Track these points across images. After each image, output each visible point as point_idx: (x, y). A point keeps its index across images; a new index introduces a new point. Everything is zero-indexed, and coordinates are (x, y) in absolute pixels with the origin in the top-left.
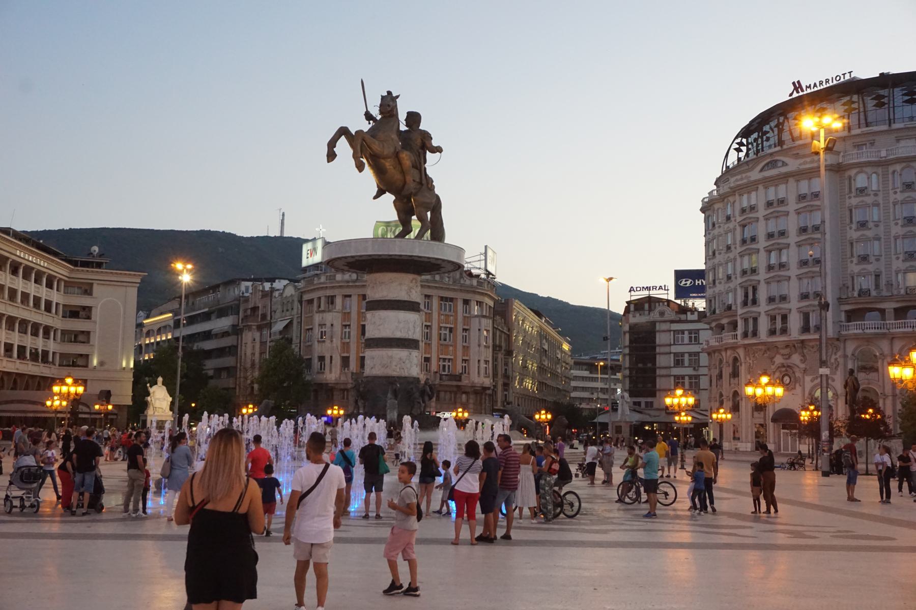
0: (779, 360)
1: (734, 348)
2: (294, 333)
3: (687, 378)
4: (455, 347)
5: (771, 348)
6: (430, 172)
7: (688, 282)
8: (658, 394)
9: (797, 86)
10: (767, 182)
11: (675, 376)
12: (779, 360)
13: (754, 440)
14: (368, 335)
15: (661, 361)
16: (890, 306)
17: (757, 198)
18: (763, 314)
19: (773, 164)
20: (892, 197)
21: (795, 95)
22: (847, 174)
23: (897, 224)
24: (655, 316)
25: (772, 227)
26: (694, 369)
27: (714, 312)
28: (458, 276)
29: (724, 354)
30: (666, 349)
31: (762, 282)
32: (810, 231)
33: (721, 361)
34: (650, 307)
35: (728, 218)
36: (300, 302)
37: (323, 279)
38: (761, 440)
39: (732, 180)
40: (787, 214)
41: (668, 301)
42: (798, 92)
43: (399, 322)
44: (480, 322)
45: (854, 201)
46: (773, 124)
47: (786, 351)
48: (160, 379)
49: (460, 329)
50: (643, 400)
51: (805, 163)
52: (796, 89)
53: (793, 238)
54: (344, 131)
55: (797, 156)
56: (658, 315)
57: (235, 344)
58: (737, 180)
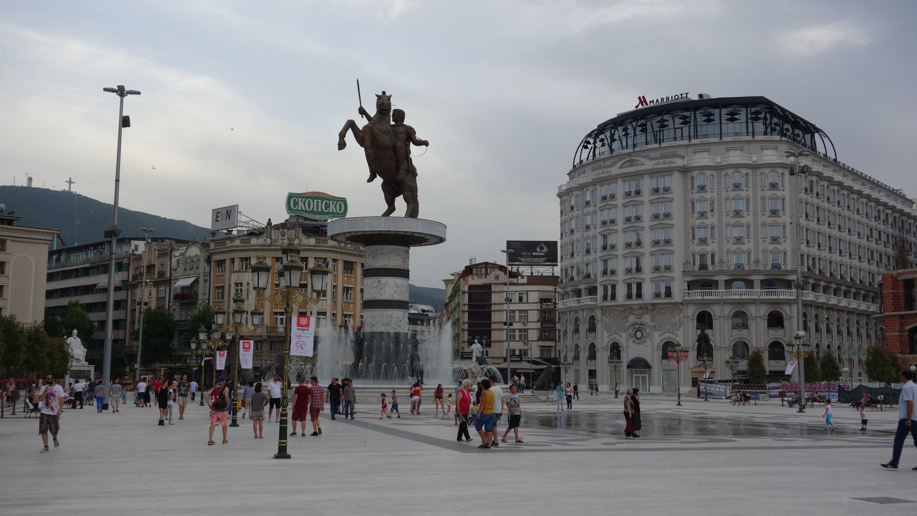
0: (632, 319)
1: (592, 309)
2: (201, 289)
3: (517, 331)
4: (354, 304)
5: (630, 308)
6: (415, 163)
9: (642, 100)
10: (625, 177)
12: (632, 319)
14: (367, 297)
15: (495, 317)
16: (721, 279)
17: (620, 188)
18: (621, 282)
19: (632, 163)
20: (724, 195)
21: (640, 106)
22: (690, 174)
23: (728, 215)
24: (490, 279)
25: (631, 212)
26: (524, 324)
27: (572, 279)
29: (581, 313)
31: (620, 257)
33: (577, 319)
34: (486, 271)
35: (588, 203)
36: (209, 260)
37: (237, 242)
39: (596, 172)
40: (642, 203)
41: (502, 268)
43: (397, 287)
45: (697, 196)
46: (620, 128)
47: (641, 311)
48: (75, 331)
49: (359, 290)
51: (658, 164)
52: (641, 102)
53: (647, 222)
54: (351, 125)
55: (653, 159)
57: (124, 298)
58: (599, 174)
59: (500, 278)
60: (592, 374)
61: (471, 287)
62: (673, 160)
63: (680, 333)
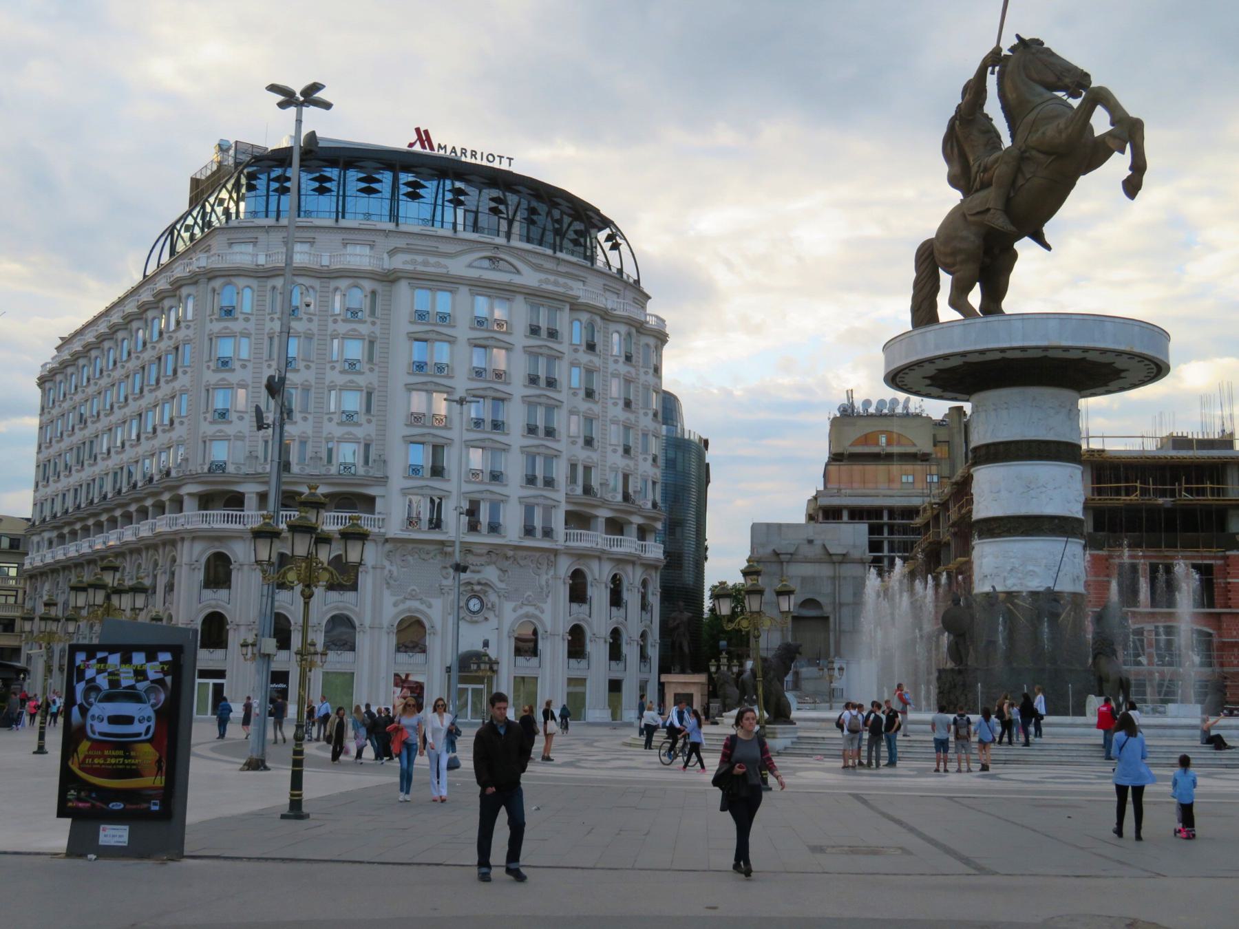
10: (480, 287)
32: (429, 370)
42: (423, 147)
51: (547, 282)
55: (538, 268)
58: (414, 262)
60: (615, 686)
62: (570, 283)
63: (548, 606)
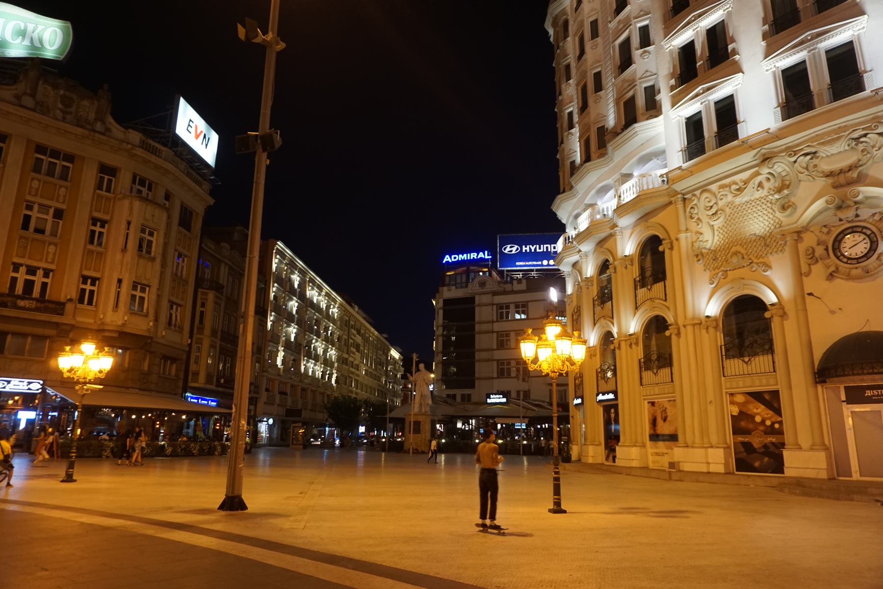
7: (514, 249)
8: (477, 382)
11: (498, 361)
13: (730, 438)
28: (92, 116)
30: (487, 327)
38: (757, 441)
44: (131, 209)
50: (459, 392)
56: (477, 287)
59: (487, 286)
61: (445, 301)
